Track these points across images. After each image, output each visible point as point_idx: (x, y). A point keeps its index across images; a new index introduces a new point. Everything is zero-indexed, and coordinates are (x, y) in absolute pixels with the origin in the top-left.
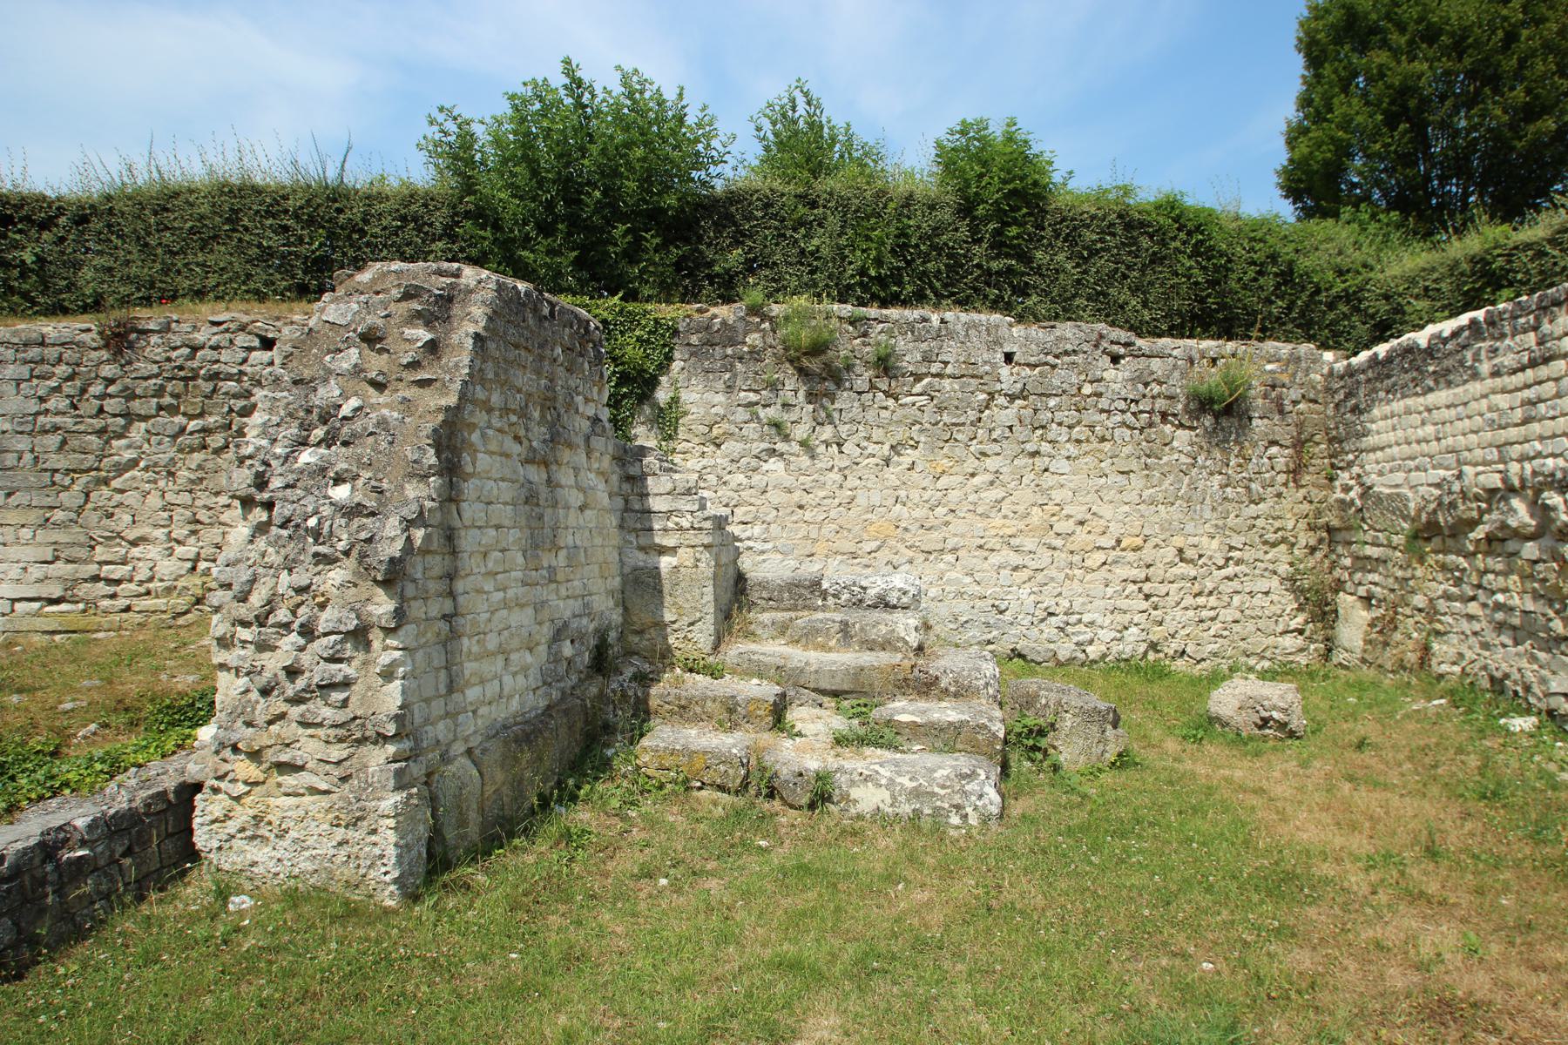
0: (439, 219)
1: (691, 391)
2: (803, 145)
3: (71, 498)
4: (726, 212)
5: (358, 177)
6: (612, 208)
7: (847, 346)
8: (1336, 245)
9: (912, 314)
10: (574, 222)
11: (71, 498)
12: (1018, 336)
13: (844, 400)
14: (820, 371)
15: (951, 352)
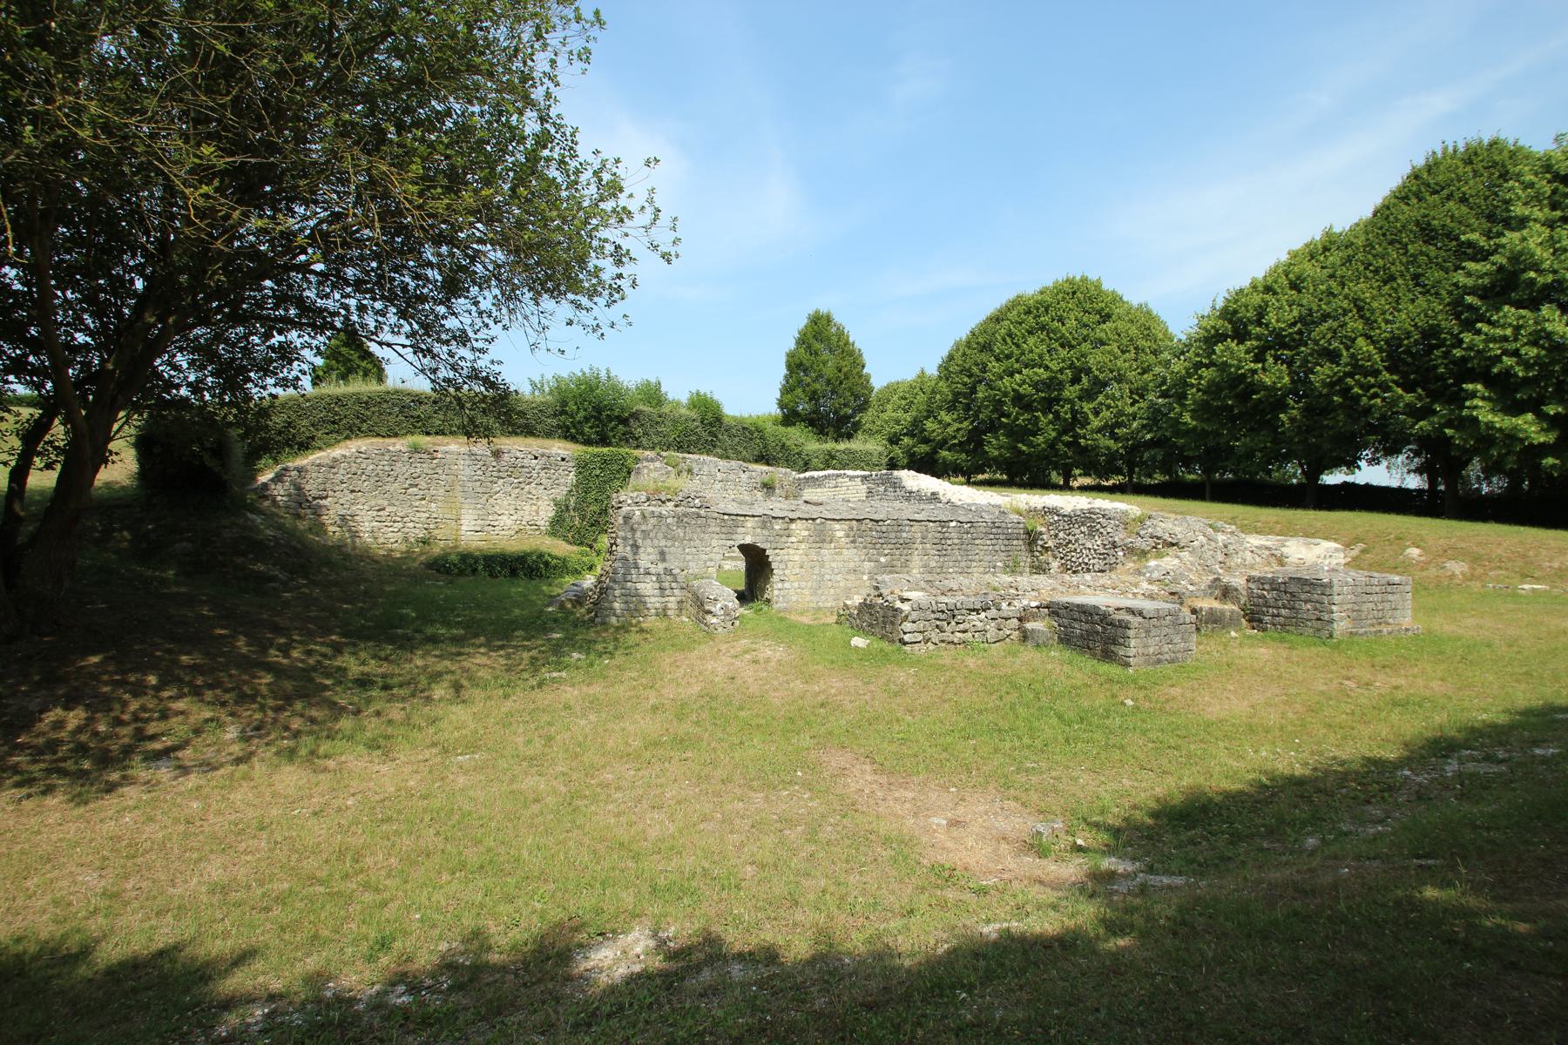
2: (652, 394)
3: (483, 500)
8: (798, 436)
11: (483, 500)
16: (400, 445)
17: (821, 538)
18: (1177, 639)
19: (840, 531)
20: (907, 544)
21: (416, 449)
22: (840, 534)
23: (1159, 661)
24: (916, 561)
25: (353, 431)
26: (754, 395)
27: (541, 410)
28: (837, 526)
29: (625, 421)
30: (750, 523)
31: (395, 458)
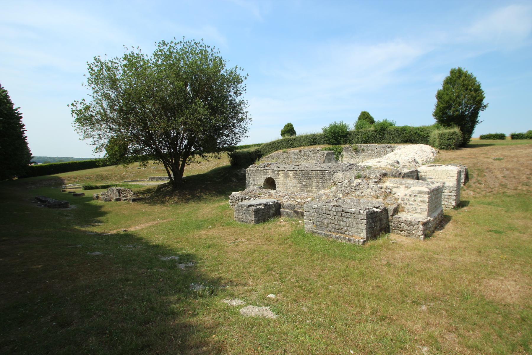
0: (323, 137)
1: (344, 153)
4: (349, 133)
5: (316, 133)
6: (338, 136)
7: (359, 148)
9: (366, 145)
10: (335, 137)
12: (377, 146)
13: (359, 154)
14: (356, 151)
15: (370, 148)
16: (281, 151)
17: (286, 176)
18: (248, 215)
19: (291, 174)
20: (311, 178)
21: (284, 152)
22: (291, 175)
23: (242, 221)
24: (314, 184)
25: (277, 149)
26: (422, 113)
27: (320, 136)
28: (290, 172)
29: (345, 136)
30: (270, 172)
31: (280, 155)
